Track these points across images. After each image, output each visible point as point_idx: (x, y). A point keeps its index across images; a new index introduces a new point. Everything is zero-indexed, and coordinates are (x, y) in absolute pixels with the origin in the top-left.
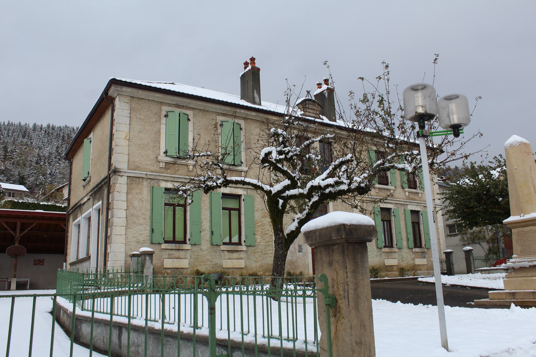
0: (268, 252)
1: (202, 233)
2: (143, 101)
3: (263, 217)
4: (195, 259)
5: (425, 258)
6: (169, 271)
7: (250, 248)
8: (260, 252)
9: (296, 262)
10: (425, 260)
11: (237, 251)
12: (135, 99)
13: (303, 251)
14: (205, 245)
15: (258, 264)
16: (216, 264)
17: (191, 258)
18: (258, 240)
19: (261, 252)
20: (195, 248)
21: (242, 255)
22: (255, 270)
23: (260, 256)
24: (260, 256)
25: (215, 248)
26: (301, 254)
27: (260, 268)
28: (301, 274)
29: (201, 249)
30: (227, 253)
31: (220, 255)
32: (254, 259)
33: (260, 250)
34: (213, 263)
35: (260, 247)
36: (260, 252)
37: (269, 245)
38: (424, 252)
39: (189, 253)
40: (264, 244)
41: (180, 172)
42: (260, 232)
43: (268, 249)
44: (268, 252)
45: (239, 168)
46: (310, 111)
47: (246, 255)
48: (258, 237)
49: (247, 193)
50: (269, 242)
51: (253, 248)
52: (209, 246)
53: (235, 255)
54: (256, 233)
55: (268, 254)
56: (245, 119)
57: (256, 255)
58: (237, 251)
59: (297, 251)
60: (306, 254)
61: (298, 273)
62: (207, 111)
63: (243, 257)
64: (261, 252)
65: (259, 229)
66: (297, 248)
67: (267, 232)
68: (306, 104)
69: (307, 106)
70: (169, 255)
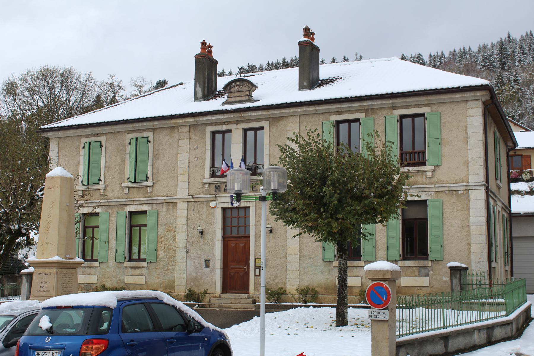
0: (171, 268)
1: (109, 252)
2: (68, 138)
3: (167, 232)
4: (103, 275)
5: (427, 275)
6: (82, 286)
7: (152, 264)
8: (162, 268)
9: (201, 278)
10: (426, 279)
11: (139, 267)
12: (62, 139)
13: (211, 266)
14: (112, 263)
15: (159, 280)
16: (120, 280)
17: (100, 274)
18: (160, 256)
19: (163, 268)
20: (102, 265)
21: (144, 271)
22: (155, 286)
23: (162, 272)
24: (162, 272)
25: (120, 265)
26: (208, 269)
27: (161, 284)
28: (206, 292)
29: (108, 266)
30: (130, 269)
31: (123, 272)
32: (156, 276)
33: (161, 266)
34: (118, 279)
35: (162, 263)
36: (162, 268)
37: (172, 261)
38: (425, 267)
39: (98, 269)
40: (167, 259)
41: (94, 198)
42: (163, 248)
43: (170, 264)
44: (171, 268)
45: (144, 184)
46: (236, 94)
47: (147, 271)
48: (161, 253)
49: (152, 208)
50: (171, 257)
51: (154, 264)
52: (115, 263)
53: (138, 271)
54: (158, 248)
55: (170, 270)
56: (154, 129)
57: (158, 271)
58: (139, 267)
59: (204, 266)
60: (214, 270)
61: (203, 291)
62: (119, 132)
63: (145, 273)
64: (163, 268)
65: (162, 245)
66: (204, 263)
67: (170, 247)
68: (231, 88)
69: (232, 90)
70: (83, 272)
